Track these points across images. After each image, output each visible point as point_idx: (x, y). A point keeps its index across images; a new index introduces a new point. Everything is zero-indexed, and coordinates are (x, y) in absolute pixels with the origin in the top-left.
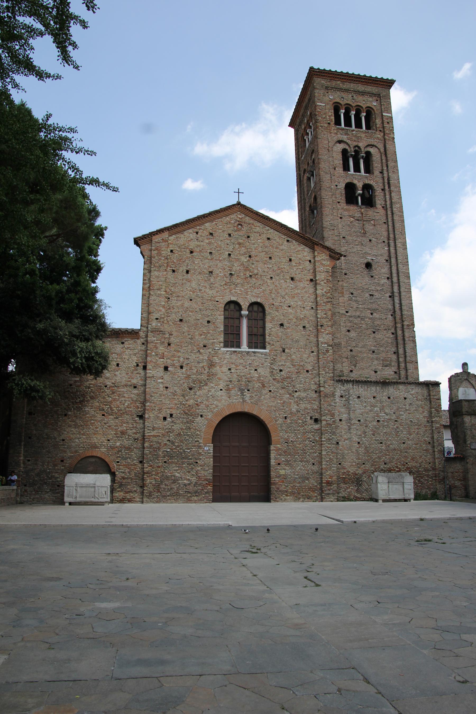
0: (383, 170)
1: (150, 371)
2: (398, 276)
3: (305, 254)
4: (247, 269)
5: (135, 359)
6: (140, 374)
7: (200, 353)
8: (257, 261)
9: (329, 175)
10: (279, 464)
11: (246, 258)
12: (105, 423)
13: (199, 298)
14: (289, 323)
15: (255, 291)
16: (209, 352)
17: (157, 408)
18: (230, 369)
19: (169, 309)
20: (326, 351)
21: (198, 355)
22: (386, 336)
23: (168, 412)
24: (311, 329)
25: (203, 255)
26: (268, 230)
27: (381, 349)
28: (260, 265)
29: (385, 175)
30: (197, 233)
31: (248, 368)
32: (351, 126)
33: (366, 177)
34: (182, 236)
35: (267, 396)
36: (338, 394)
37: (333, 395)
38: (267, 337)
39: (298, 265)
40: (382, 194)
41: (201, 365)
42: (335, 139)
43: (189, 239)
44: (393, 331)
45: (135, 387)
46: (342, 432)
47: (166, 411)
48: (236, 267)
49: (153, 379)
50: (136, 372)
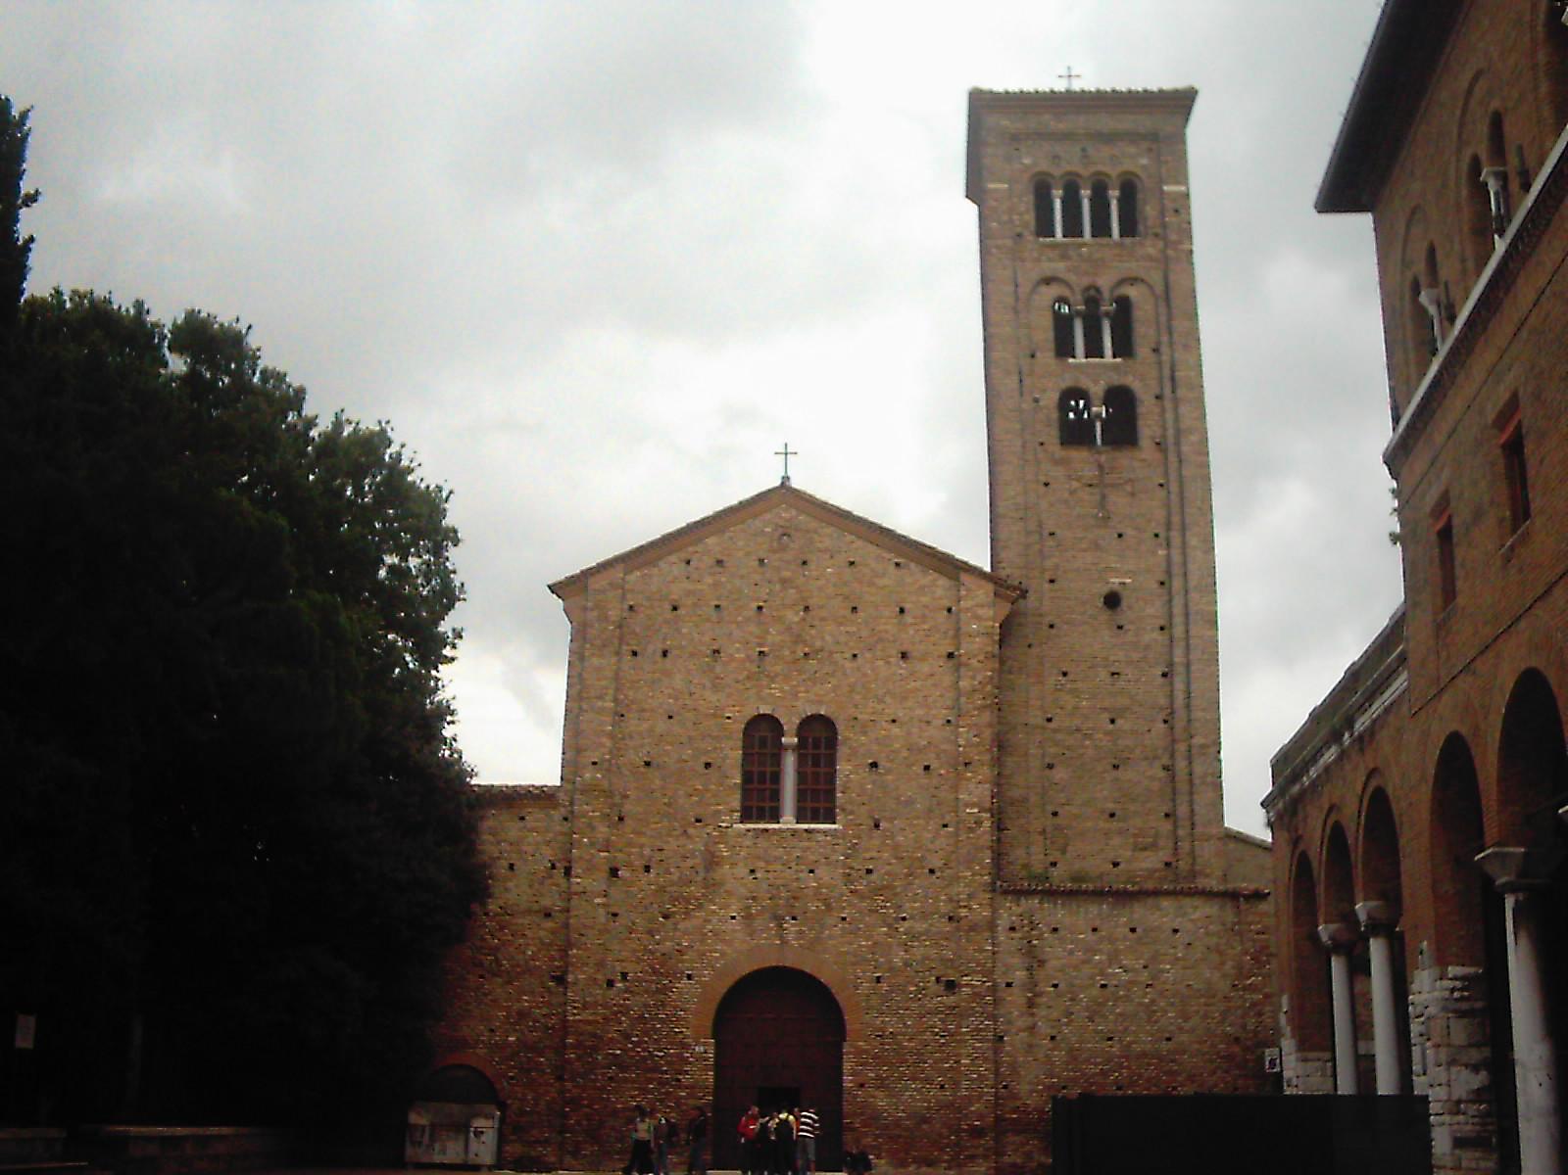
0: (1159, 343)
1: (579, 880)
2: (1187, 624)
3: (939, 592)
4: (798, 639)
5: (548, 853)
6: (557, 885)
7: (689, 837)
8: (823, 619)
9: (1016, 378)
10: (862, 1085)
11: (797, 613)
12: (486, 995)
13: (689, 711)
14: (892, 761)
15: (817, 689)
16: (708, 834)
17: (592, 961)
18: (752, 871)
19: (623, 739)
20: (975, 823)
21: (683, 841)
22: (1145, 776)
23: (618, 969)
24: (942, 772)
25: (700, 612)
26: (853, 542)
27: (1132, 808)
28: (830, 627)
29: (1165, 358)
30: (688, 562)
31: (795, 867)
32: (1081, 234)
33: (1115, 367)
34: (655, 571)
35: (837, 931)
36: (1003, 923)
37: (992, 926)
38: (839, 795)
39: (918, 620)
40: (1157, 410)
41: (690, 863)
42: (1035, 276)
43: (669, 578)
44: (1165, 761)
45: (548, 915)
46: (1011, 1013)
47: (614, 967)
48: (774, 635)
49: (584, 897)
50: (550, 881)
